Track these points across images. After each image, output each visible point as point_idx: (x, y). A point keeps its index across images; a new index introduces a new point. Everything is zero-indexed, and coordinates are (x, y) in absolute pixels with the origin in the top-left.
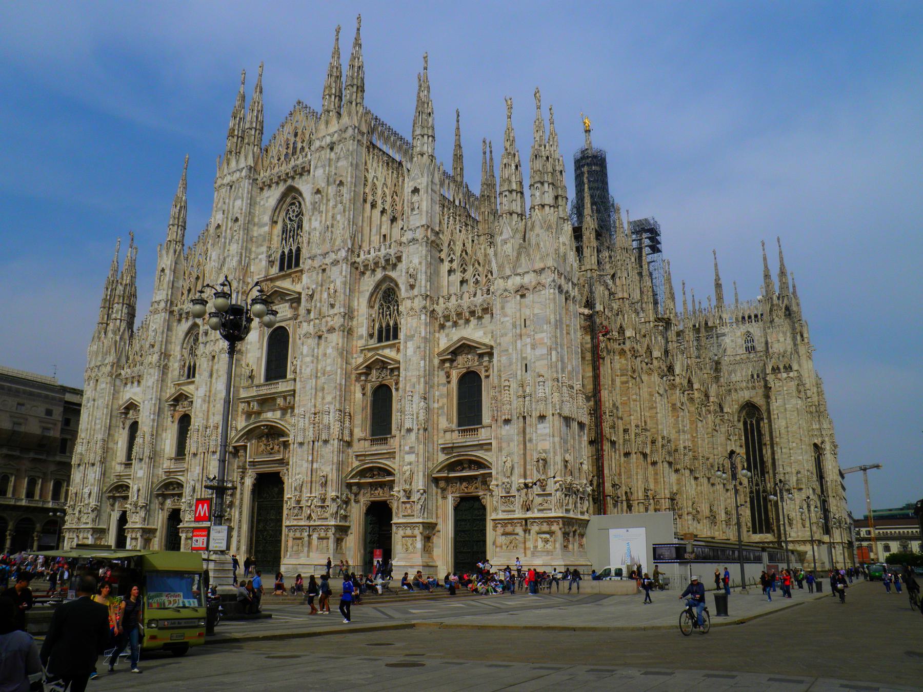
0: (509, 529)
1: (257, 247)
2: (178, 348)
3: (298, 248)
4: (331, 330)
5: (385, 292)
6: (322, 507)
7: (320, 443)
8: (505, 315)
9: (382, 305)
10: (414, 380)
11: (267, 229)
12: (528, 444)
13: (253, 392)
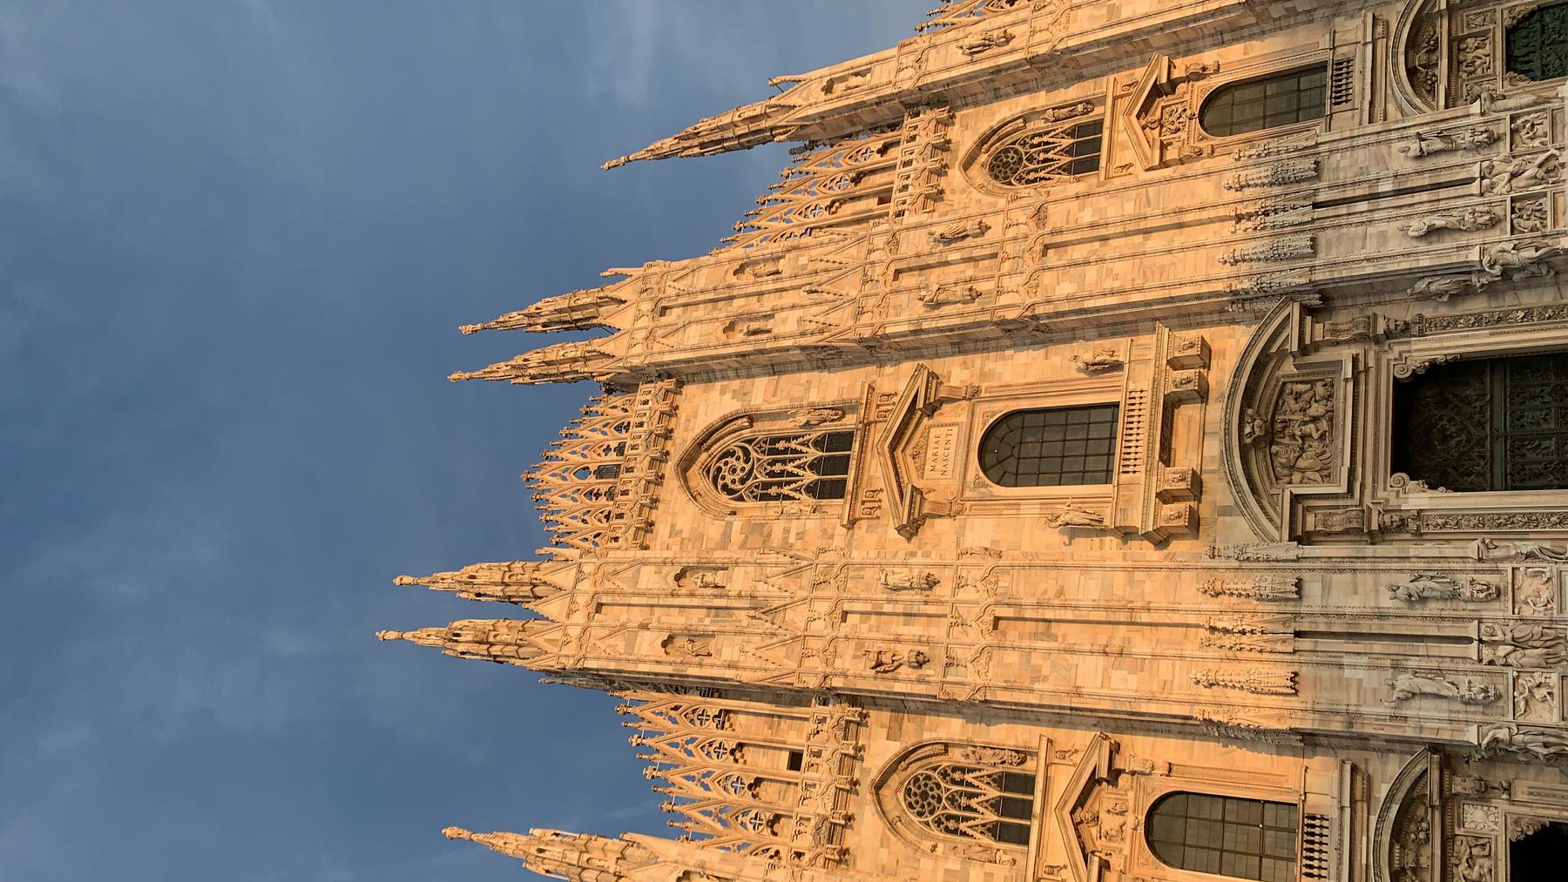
2: (926, 863)
3: (818, 444)
4: (1040, 215)
5: (996, 178)
7: (1320, 185)
9: (1019, 180)
11: (737, 523)
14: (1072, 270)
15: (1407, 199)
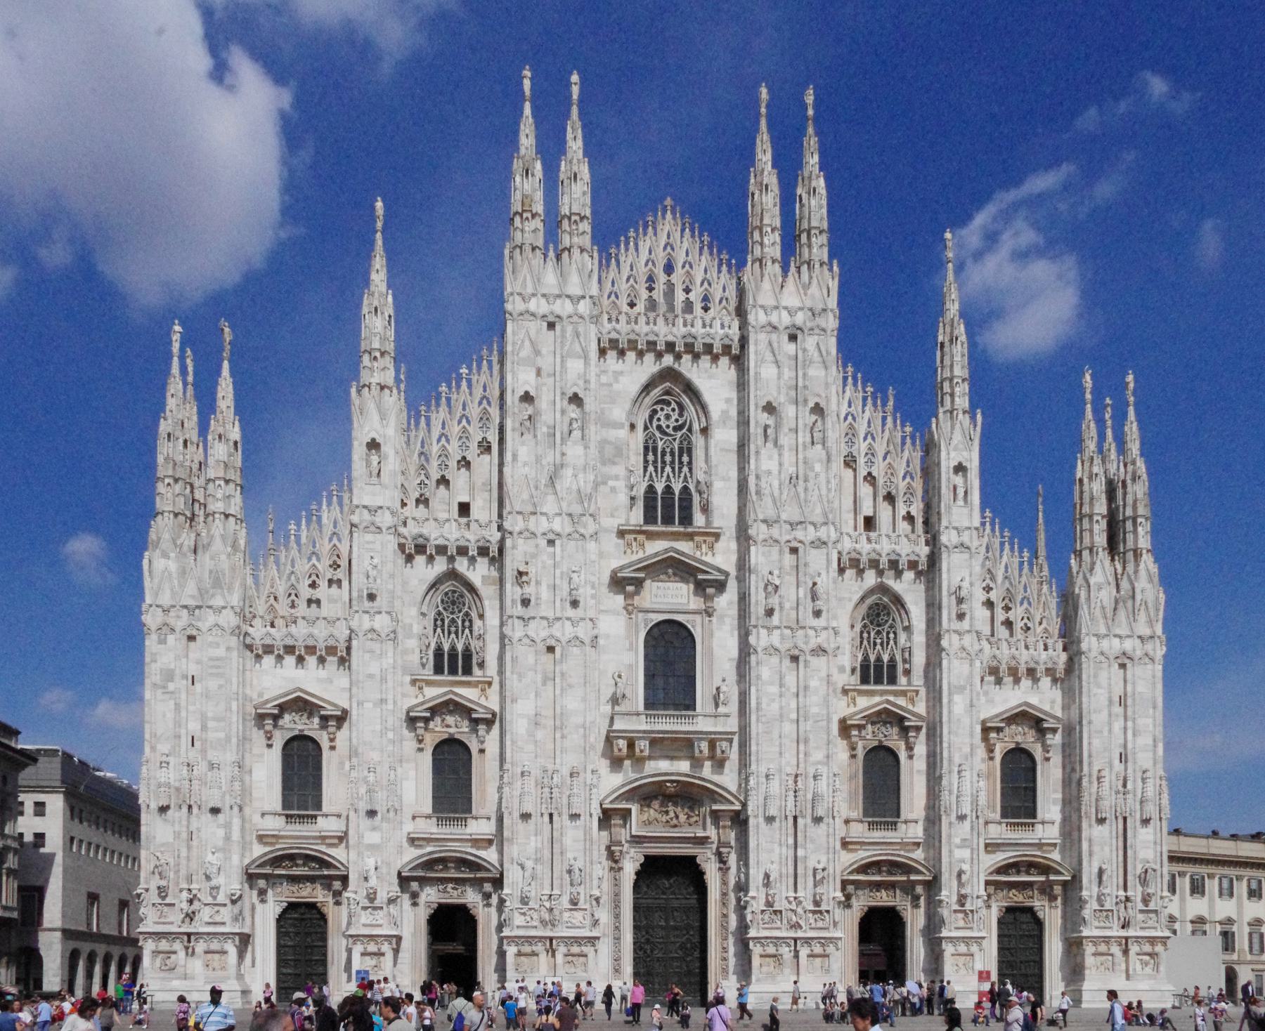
0: (1103, 948)
1: (604, 464)
2: (414, 611)
4: (820, 651)
6: (814, 912)
8: (1099, 686)
10: (967, 750)
11: (623, 433)
12: (1129, 852)
13: (641, 724)
14: (777, 677)
15: (791, 863)
